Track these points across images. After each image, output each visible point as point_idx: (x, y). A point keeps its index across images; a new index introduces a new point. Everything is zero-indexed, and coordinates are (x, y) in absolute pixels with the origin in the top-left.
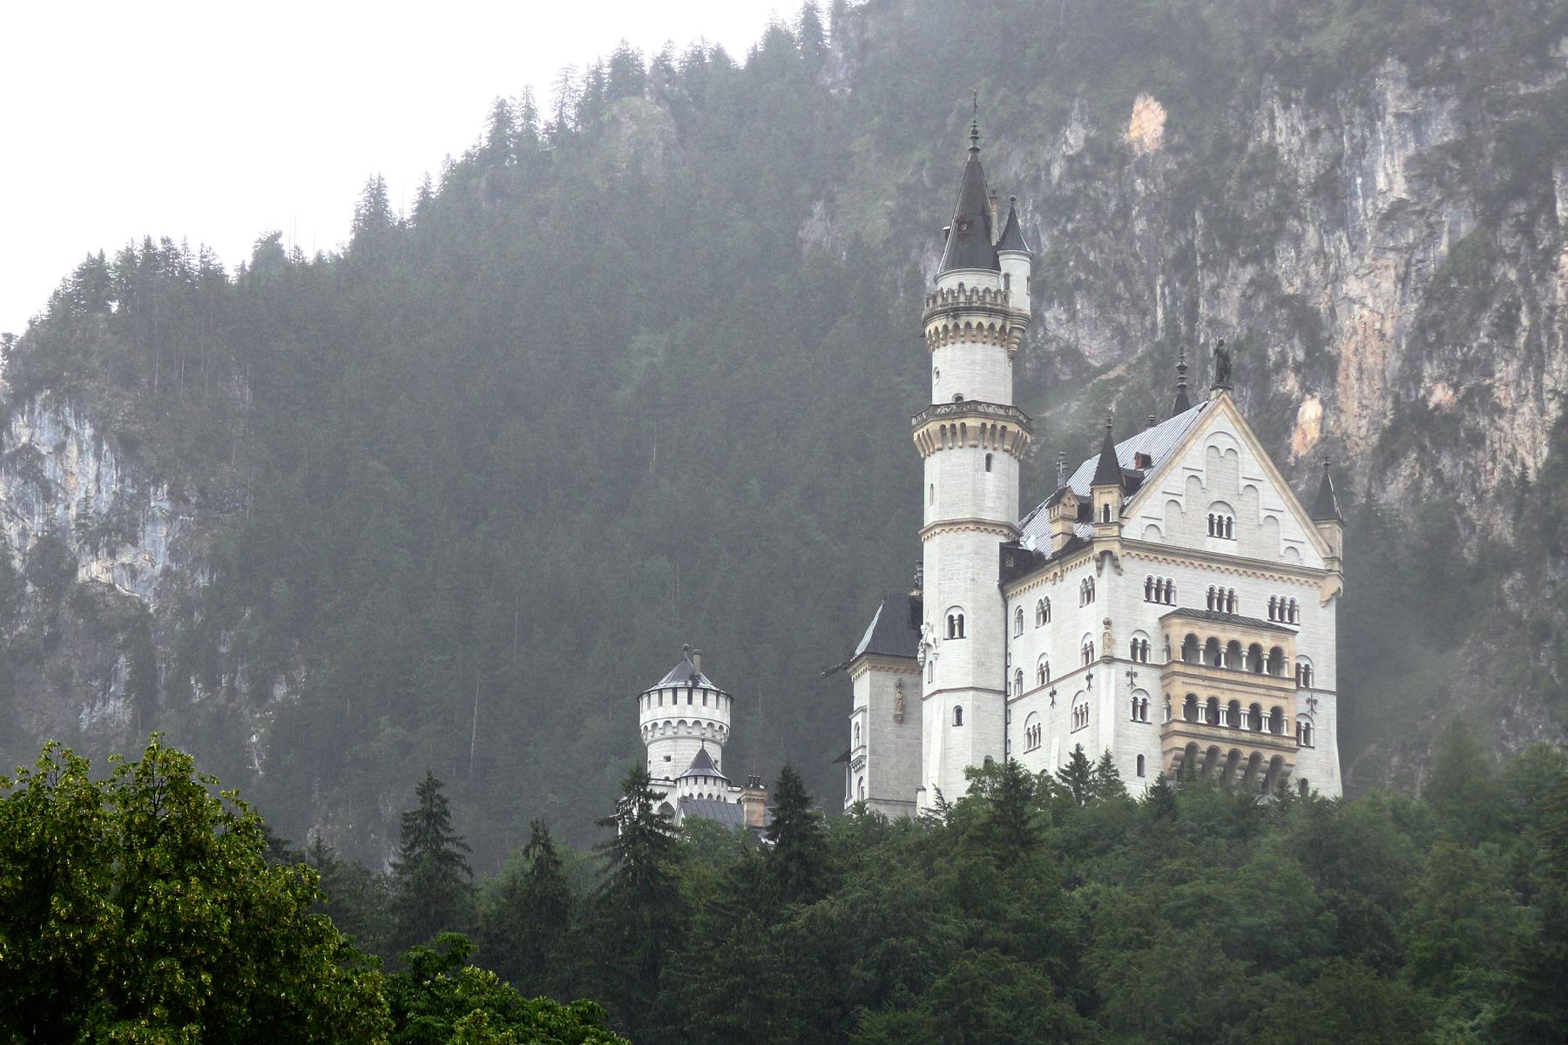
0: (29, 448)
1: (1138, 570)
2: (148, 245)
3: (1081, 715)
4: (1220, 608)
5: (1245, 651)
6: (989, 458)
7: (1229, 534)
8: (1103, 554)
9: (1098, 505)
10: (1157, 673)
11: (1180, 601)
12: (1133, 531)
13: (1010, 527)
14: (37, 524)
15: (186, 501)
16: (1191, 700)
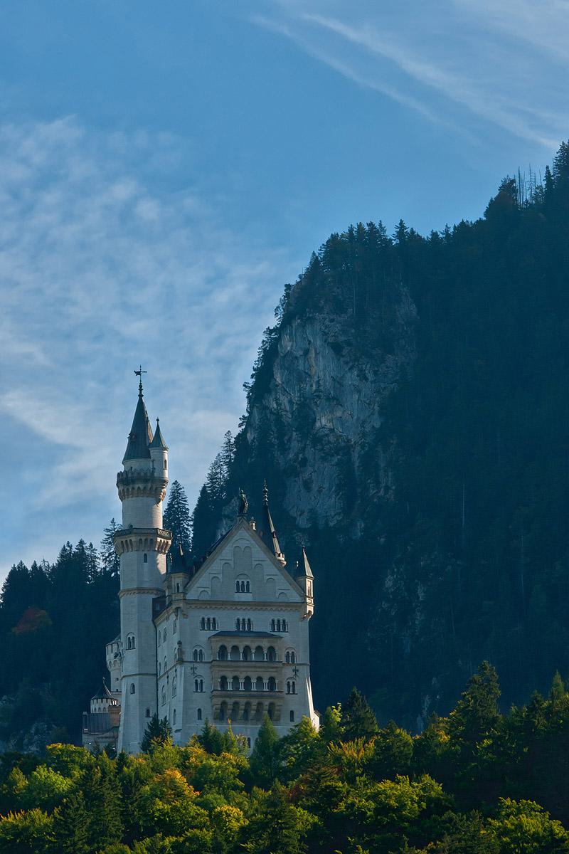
0: (290, 353)
1: (197, 615)
2: (360, 226)
3: (175, 689)
4: (244, 628)
5: (253, 651)
6: (145, 555)
7: (248, 591)
8: (177, 609)
9: (174, 583)
10: (209, 665)
11: (220, 628)
12: (192, 595)
13: (158, 590)
14: (296, 397)
15: (366, 379)
16: (224, 679)
